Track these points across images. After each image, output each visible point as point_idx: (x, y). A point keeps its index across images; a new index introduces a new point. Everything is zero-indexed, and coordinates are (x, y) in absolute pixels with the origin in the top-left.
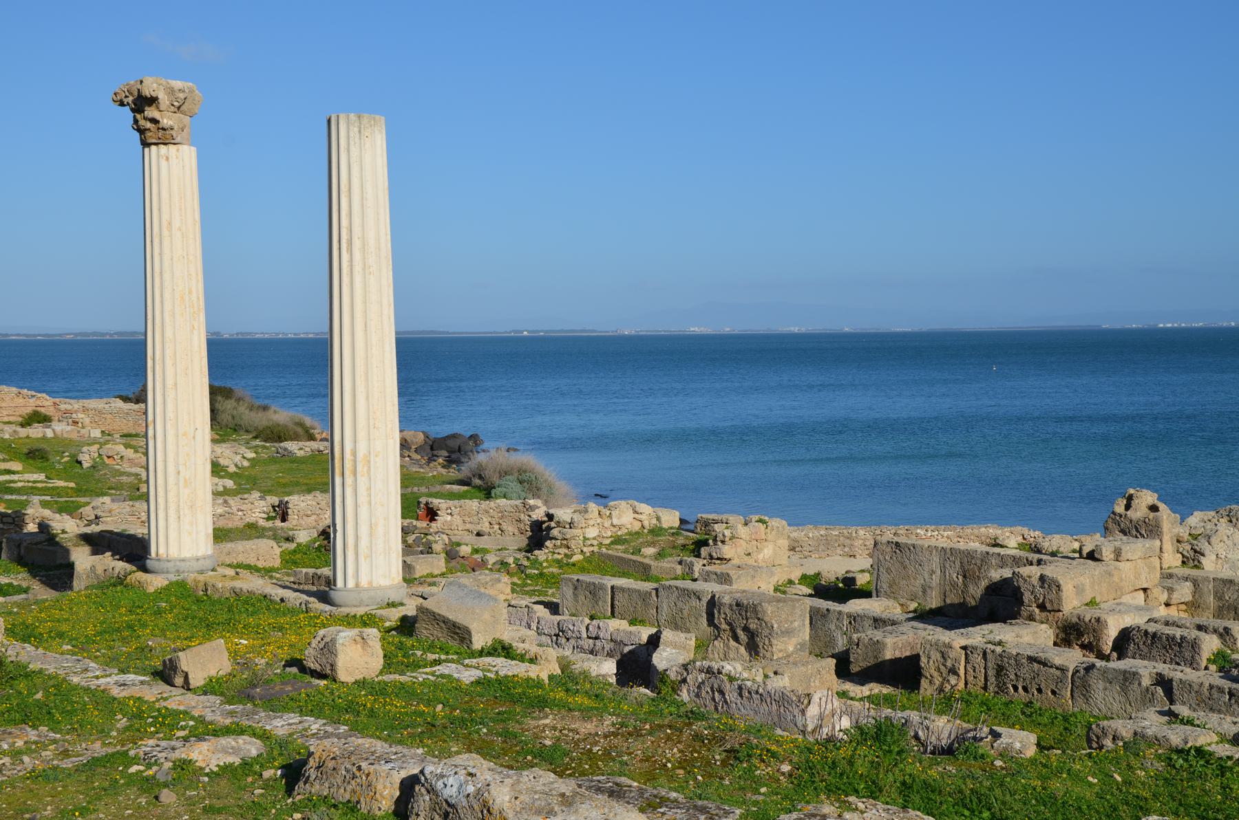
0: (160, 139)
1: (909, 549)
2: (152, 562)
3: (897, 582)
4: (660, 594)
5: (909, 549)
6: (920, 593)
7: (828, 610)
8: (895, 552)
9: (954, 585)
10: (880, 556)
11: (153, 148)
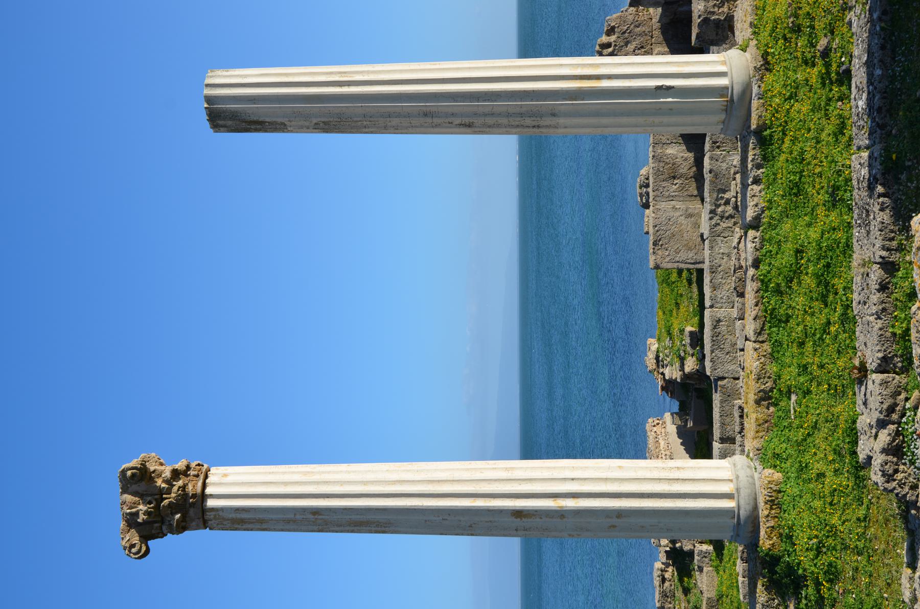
0: (197, 476)
1: (658, 231)
2: (742, 502)
3: (686, 242)
4: (721, 375)
5: (658, 231)
6: (693, 219)
7: (710, 172)
8: (662, 245)
9: (682, 188)
10: (667, 259)
11: (208, 491)
